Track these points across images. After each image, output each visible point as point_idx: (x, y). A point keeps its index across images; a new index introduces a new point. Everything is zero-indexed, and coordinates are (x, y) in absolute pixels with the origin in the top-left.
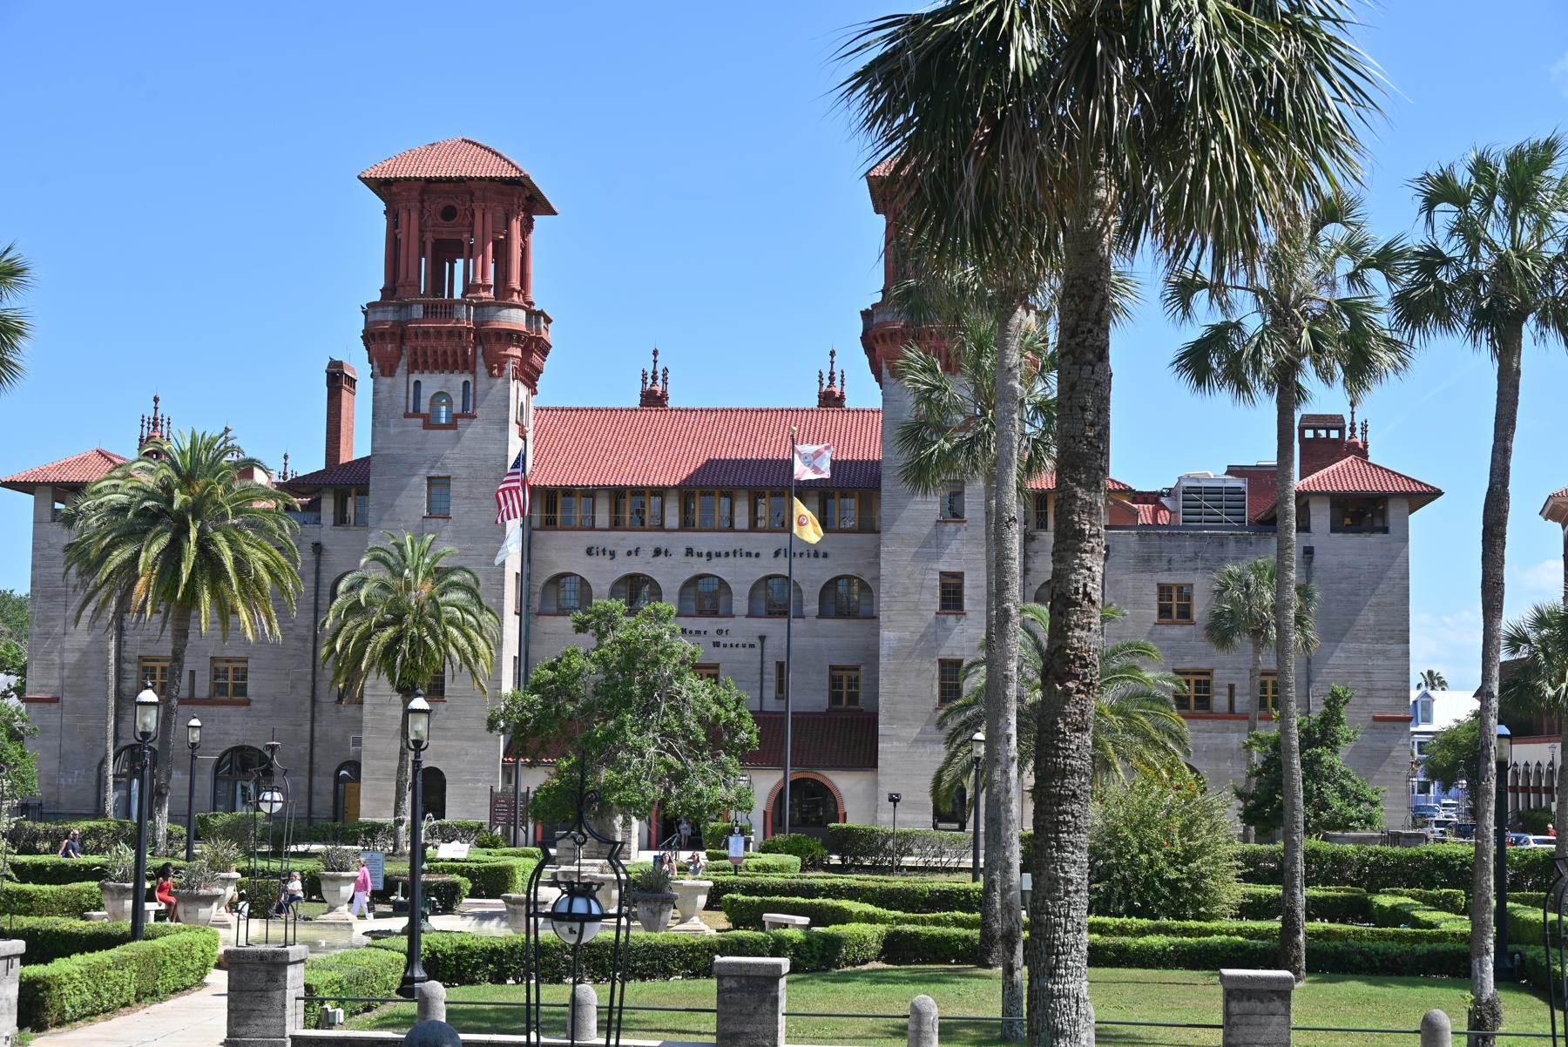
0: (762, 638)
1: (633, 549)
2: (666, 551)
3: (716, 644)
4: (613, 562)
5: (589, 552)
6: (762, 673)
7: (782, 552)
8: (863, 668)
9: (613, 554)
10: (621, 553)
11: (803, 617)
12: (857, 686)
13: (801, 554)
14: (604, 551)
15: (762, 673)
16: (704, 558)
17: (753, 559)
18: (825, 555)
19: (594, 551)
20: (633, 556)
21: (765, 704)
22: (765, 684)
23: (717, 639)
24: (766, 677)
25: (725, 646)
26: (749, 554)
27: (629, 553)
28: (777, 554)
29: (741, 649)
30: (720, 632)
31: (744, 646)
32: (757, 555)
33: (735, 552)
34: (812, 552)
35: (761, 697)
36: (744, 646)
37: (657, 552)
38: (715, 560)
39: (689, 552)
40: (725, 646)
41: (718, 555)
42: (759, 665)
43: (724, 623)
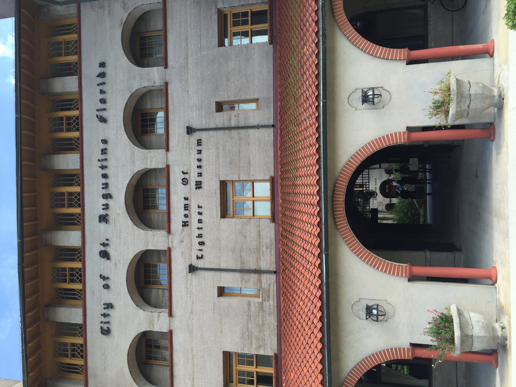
0: (190, 131)
1: (103, 283)
2: (104, 245)
3: (199, 185)
4: (116, 305)
5: (106, 332)
6: (230, 128)
7: (101, 114)
8: (220, 6)
9: (109, 306)
10: (108, 297)
11: (166, 84)
12: (245, 14)
13: (102, 92)
14: (105, 315)
15: (230, 128)
16: (110, 202)
17: (109, 146)
18: (102, 65)
19: (105, 326)
20: (109, 282)
21: (266, 123)
22: (242, 124)
23: (193, 185)
24: (233, 124)
25: (200, 175)
26: (104, 151)
27: (106, 287)
28: (103, 120)
29: (203, 156)
30: (185, 182)
31: (200, 152)
32: (105, 142)
33: (103, 167)
34: (100, 80)
35: (258, 127)
36: (200, 152)
37: (105, 255)
38: (112, 190)
39: (103, 219)
40: (200, 175)
41: (106, 186)
42: (220, 133)
43: (176, 177)
